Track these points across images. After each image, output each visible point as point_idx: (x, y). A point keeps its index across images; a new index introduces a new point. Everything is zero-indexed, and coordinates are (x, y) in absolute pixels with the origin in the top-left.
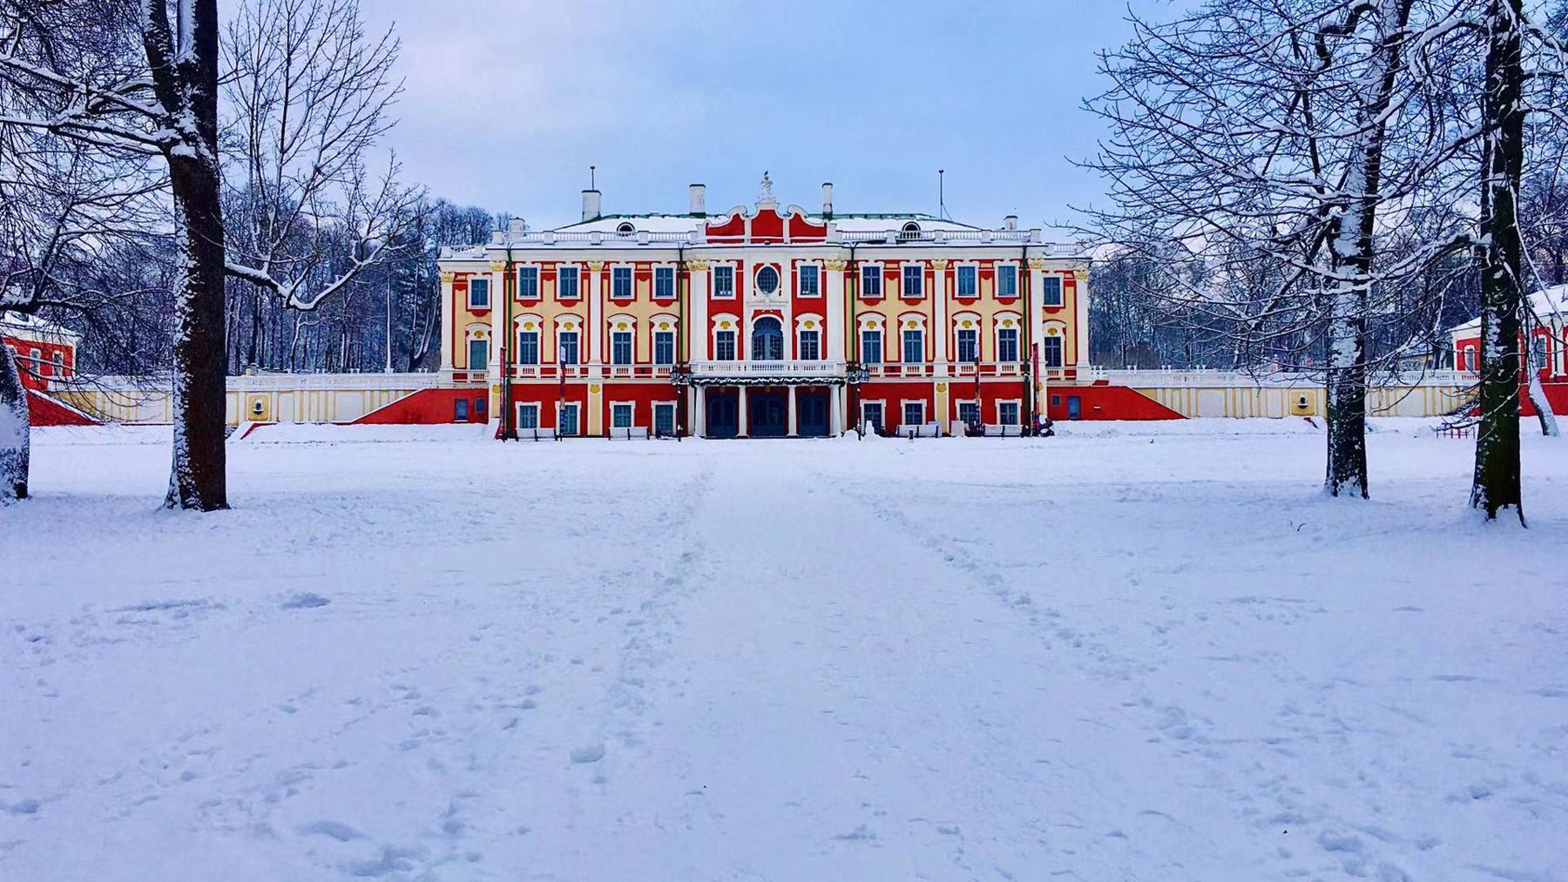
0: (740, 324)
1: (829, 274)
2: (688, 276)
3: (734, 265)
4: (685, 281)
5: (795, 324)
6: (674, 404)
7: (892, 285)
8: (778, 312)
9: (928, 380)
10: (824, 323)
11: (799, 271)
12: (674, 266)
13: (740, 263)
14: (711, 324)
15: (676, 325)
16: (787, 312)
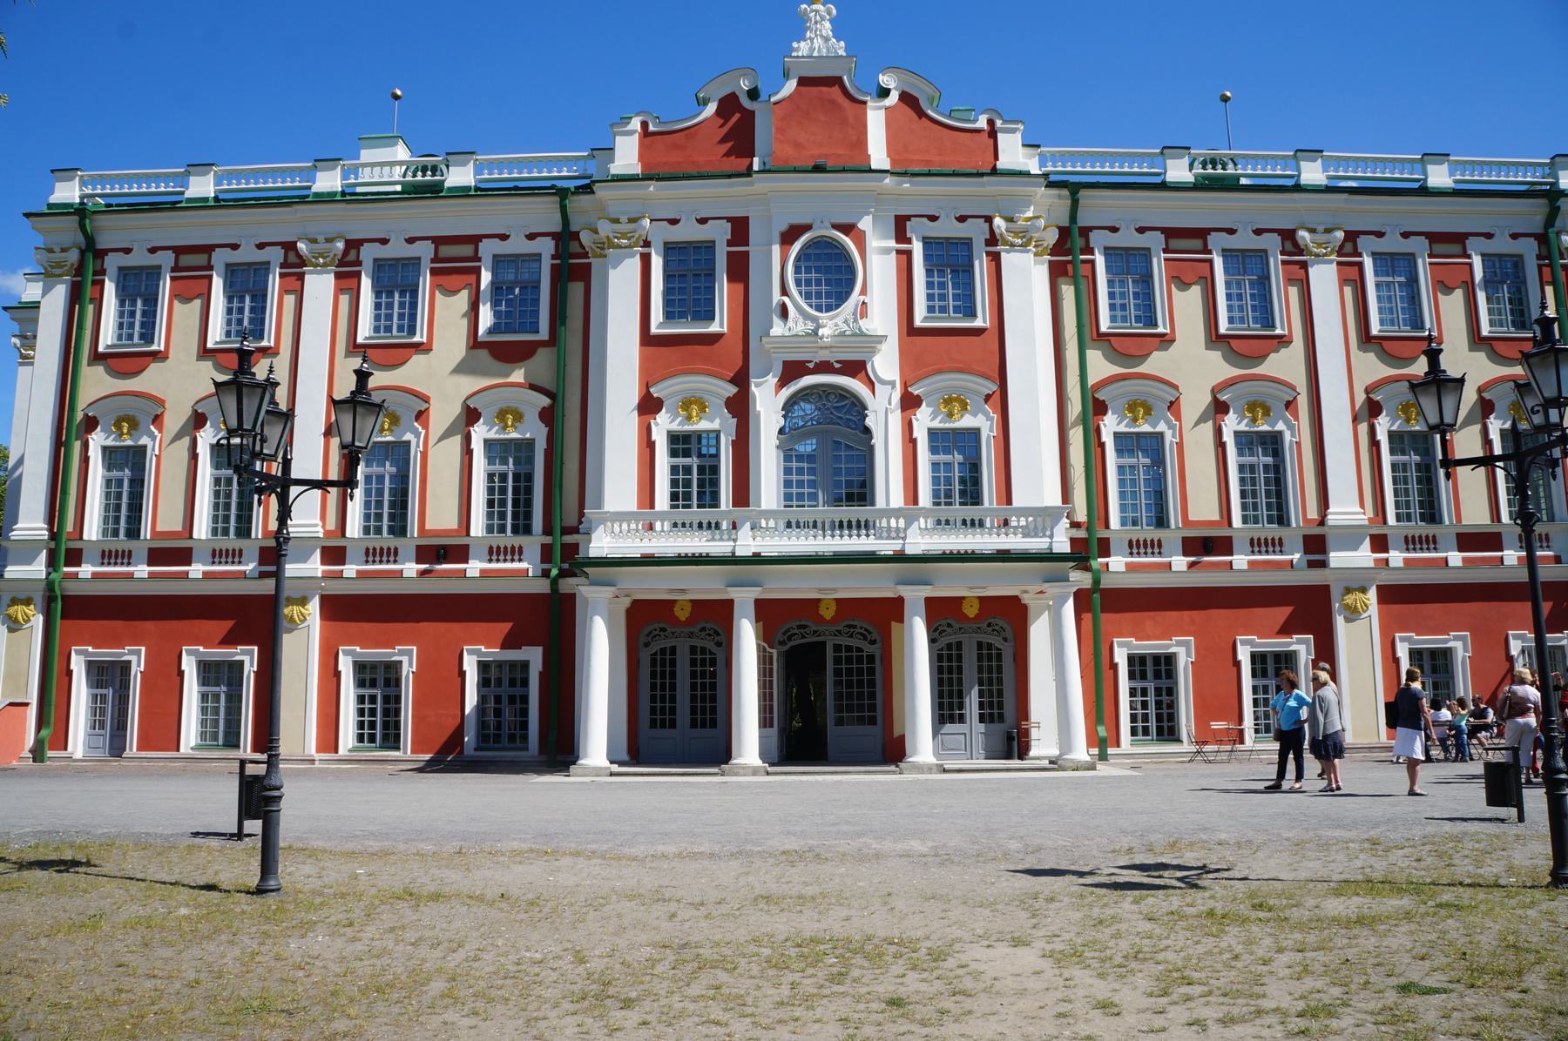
0: (740, 407)
1: (1009, 260)
2: (584, 274)
3: (720, 233)
4: (576, 289)
5: (910, 403)
6: (533, 656)
7: (1188, 302)
8: (855, 368)
9: (1313, 577)
10: (1000, 401)
11: (917, 248)
12: (546, 247)
13: (740, 229)
14: (649, 406)
15: (547, 416)
16: (886, 364)
